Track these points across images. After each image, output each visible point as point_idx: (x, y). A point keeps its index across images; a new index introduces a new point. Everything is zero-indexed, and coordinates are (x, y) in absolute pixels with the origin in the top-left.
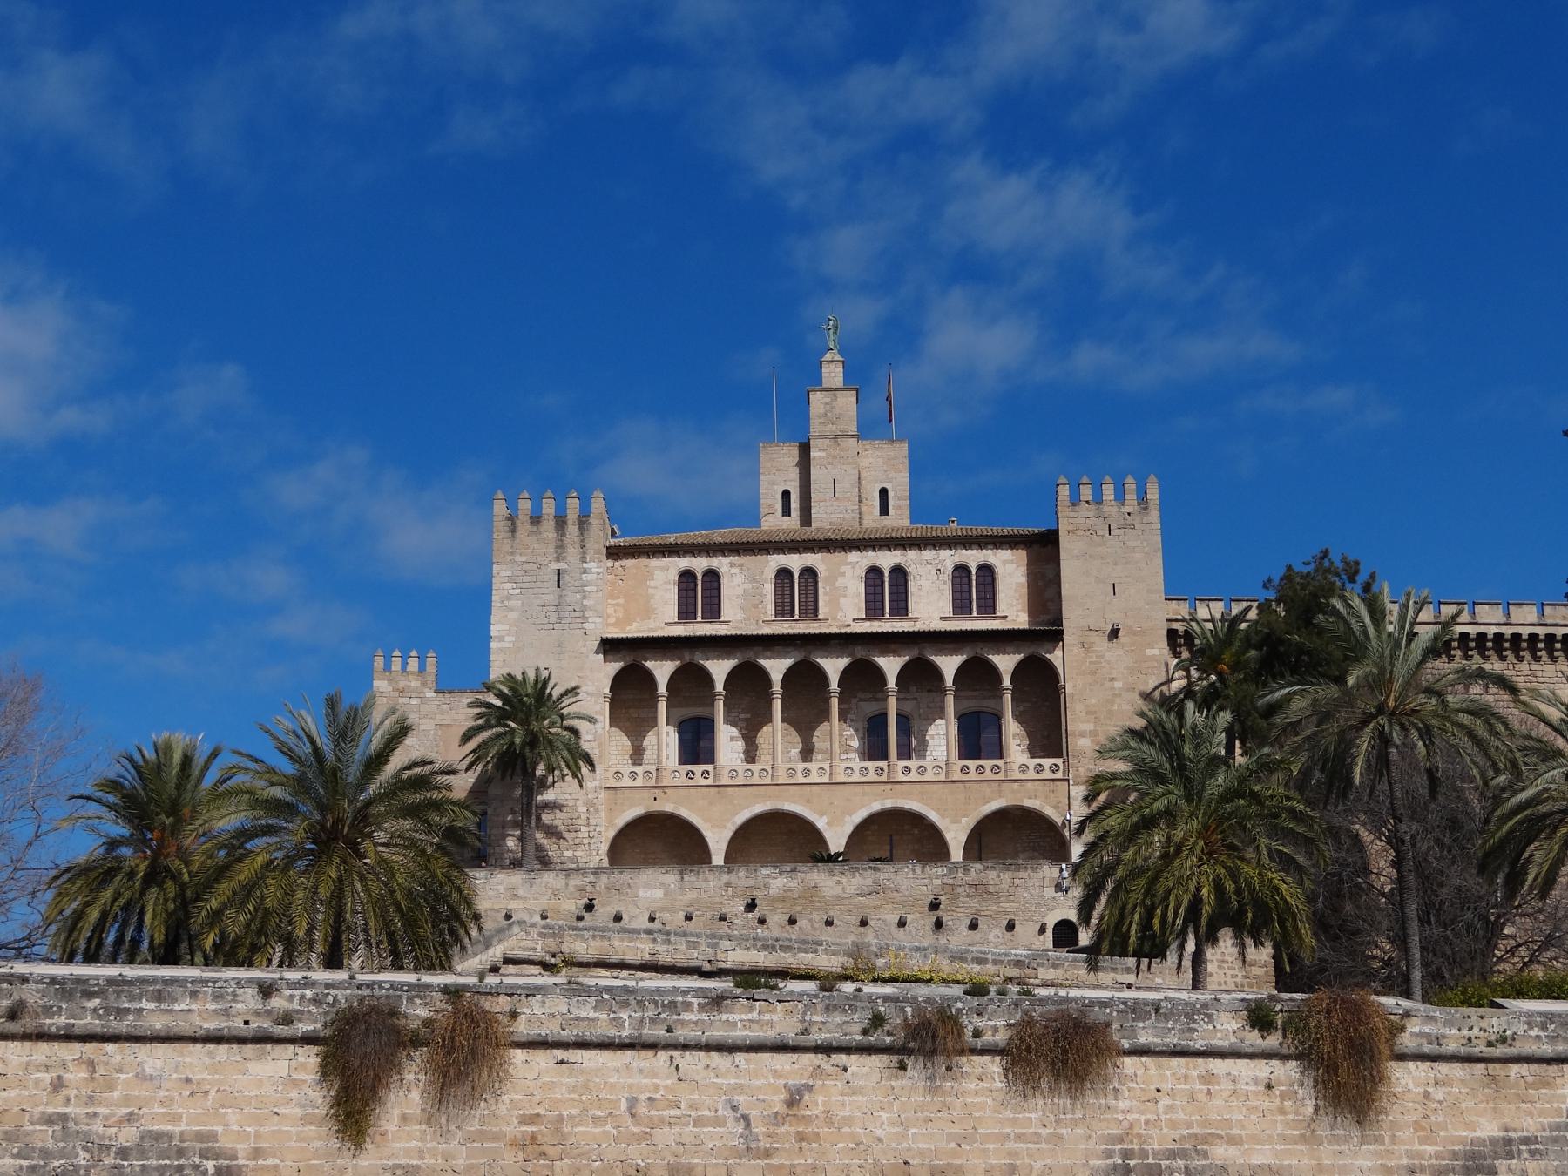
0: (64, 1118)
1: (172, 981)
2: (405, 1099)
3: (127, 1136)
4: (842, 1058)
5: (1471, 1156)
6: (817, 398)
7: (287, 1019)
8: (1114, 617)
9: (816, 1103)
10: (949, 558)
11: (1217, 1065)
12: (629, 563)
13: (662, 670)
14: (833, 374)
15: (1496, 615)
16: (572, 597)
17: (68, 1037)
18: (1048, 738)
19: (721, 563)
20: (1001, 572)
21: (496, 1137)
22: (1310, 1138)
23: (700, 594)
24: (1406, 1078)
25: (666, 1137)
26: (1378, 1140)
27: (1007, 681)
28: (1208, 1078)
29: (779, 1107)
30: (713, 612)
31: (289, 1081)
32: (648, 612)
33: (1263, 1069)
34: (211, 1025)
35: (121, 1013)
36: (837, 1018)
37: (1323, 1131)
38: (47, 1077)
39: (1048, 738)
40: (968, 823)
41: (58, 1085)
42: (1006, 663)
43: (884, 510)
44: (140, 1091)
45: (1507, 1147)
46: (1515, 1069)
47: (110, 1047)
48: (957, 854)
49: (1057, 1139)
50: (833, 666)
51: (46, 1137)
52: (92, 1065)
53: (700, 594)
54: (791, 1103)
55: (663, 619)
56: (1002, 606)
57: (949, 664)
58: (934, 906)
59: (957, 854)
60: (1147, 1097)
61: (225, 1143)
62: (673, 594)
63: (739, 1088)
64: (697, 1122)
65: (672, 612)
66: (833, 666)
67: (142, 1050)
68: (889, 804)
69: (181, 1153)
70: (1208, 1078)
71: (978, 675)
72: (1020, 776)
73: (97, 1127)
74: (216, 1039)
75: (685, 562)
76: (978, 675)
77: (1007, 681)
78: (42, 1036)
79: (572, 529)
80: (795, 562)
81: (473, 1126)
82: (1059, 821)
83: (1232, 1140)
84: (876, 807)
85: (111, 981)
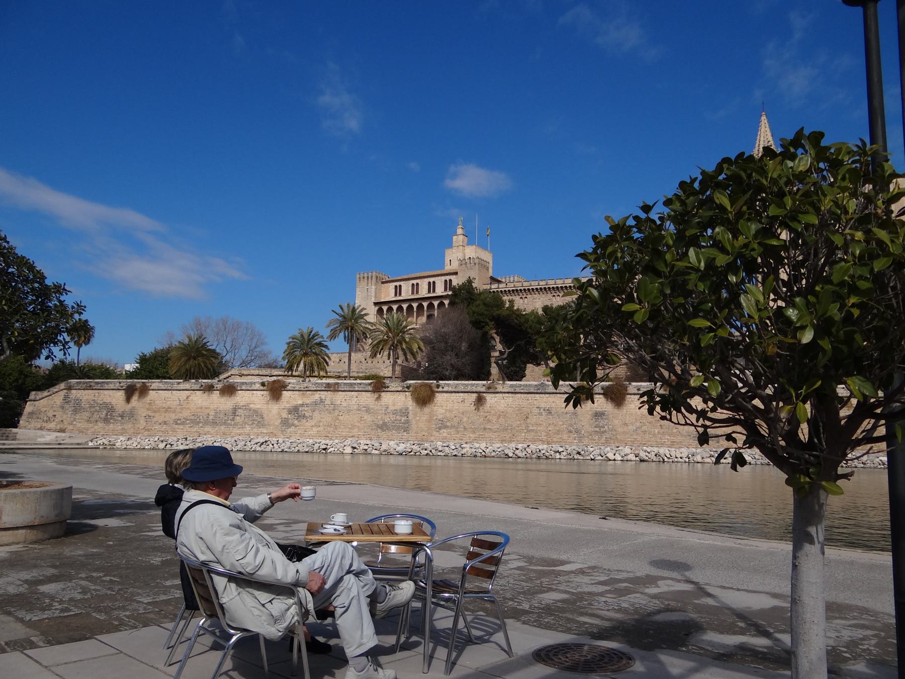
2: (135, 398)
6: (455, 237)
9: (190, 398)
10: (443, 278)
13: (385, 308)
14: (460, 231)
15: (561, 282)
19: (402, 283)
22: (267, 404)
23: (398, 291)
31: (121, 395)
32: (388, 295)
33: (262, 393)
45: (302, 405)
53: (398, 291)
55: (391, 297)
60: (242, 397)
62: (394, 291)
80: (415, 282)
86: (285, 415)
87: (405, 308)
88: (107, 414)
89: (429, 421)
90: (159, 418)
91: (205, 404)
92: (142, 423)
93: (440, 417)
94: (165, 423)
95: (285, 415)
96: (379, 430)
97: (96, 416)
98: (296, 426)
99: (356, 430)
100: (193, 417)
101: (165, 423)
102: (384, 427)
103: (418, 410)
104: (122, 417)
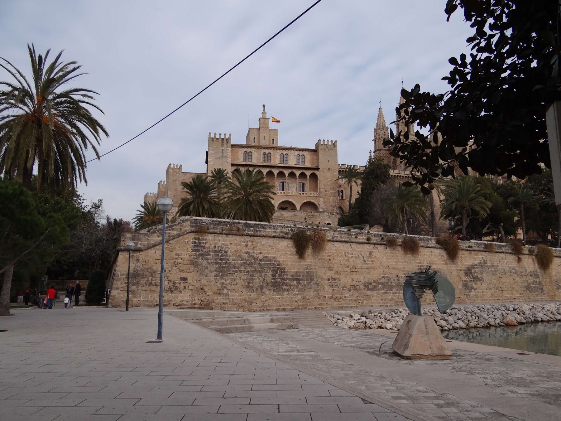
0: (249, 252)
1: (265, 225)
2: (309, 251)
3: (260, 257)
4: (377, 246)
5: (468, 268)
7: (287, 234)
8: (329, 167)
9: (374, 254)
10: (297, 153)
11: (432, 250)
12: (234, 149)
16: (225, 155)
17: (248, 235)
18: (315, 188)
20: (306, 156)
21: (324, 259)
22: (446, 264)
24: (460, 253)
25: (351, 260)
26: (455, 264)
27: (308, 177)
28: (431, 252)
29: (368, 255)
30: (251, 160)
34: (274, 234)
35: (257, 231)
36: (376, 238)
37: (448, 263)
38: (245, 244)
39: (315, 188)
40: (301, 204)
41: (247, 246)
42: (308, 173)
43: (273, 143)
44: (262, 248)
45: (473, 266)
46: (473, 252)
47: (255, 238)
48: (298, 209)
49: (410, 263)
50: (276, 171)
51: (246, 256)
52: (252, 242)
53: (248, 156)
54: (370, 254)
55: (241, 161)
56: (306, 163)
57: (298, 173)
58: (305, 219)
59: (298, 209)
61: (278, 259)
62: (243, 156)
63: (361, 251)
64: (356, 258)
65: (242, 160)
66: (276, 171)
67: (261, 239)
68: (286, 199)
69: (270, 261)
70: (431, 252)
71: (303, 175)
72: (310, 196)
73: (255, 255)
74: (274, 237)
75: (245, 150)
76: (303, 175)
77: (308, 177)
78: (243, 235)
79: (225, 141)
80: (267, 151)
81: (320, 257)
82: (317, 204)
83: (436, 264)
84: (284, 200)
85: (255, 224)
86: (464, 278)
87: (265, 174)
88: (274, 277)
89: (551, 282)
90: (346, 280)
91: (391, 262)
92: (327, 290)
93: (555, 278)
94: (355, 288)
95: (464, 278)
96: (528, 292)
97: (258, 281)
98: (475, 289)
99: (514, 292)
100: (383, 280)
101: (355, 288)
102: (528, 288)
103: (543, 272)
104: (297, 280)
